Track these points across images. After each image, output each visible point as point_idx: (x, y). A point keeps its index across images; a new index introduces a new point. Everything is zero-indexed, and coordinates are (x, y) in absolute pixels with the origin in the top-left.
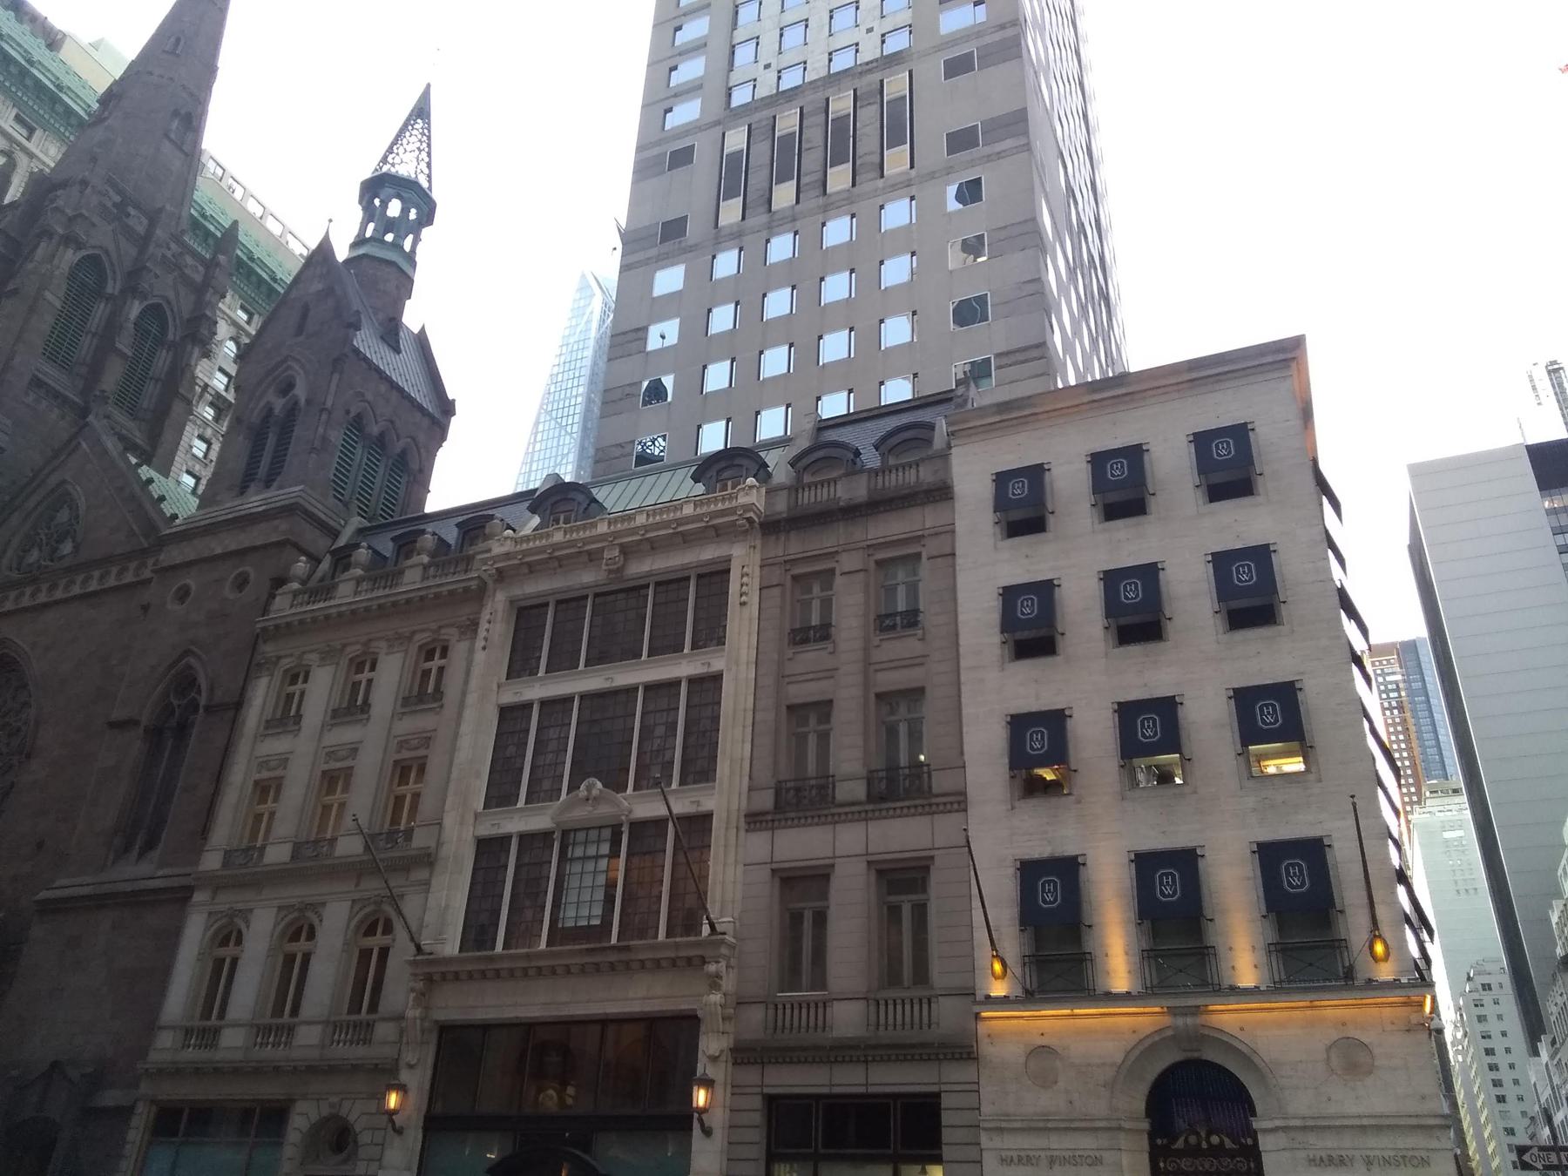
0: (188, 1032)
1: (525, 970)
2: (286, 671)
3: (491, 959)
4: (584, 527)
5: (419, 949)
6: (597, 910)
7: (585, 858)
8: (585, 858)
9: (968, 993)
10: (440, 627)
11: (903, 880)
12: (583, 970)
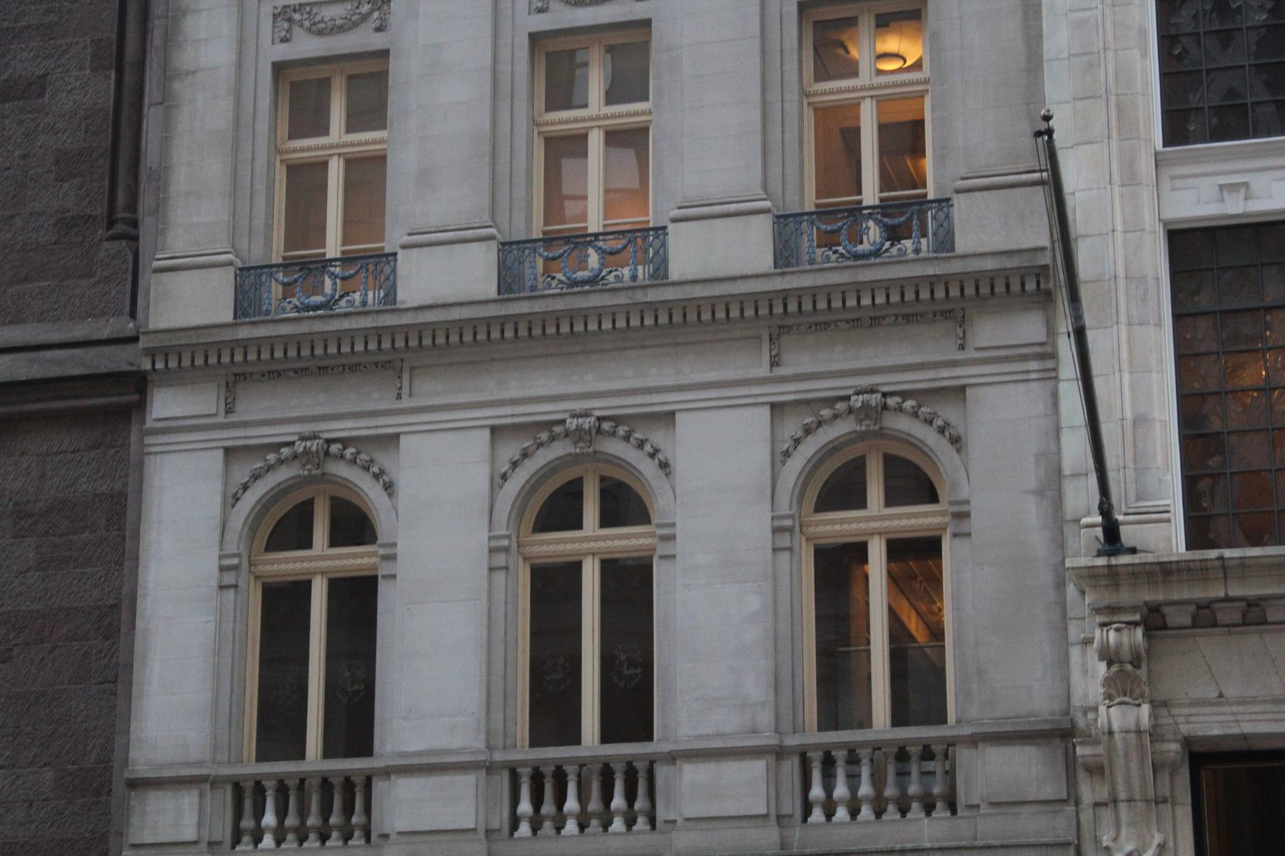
0: (246, 796)
5: (1111, 531)
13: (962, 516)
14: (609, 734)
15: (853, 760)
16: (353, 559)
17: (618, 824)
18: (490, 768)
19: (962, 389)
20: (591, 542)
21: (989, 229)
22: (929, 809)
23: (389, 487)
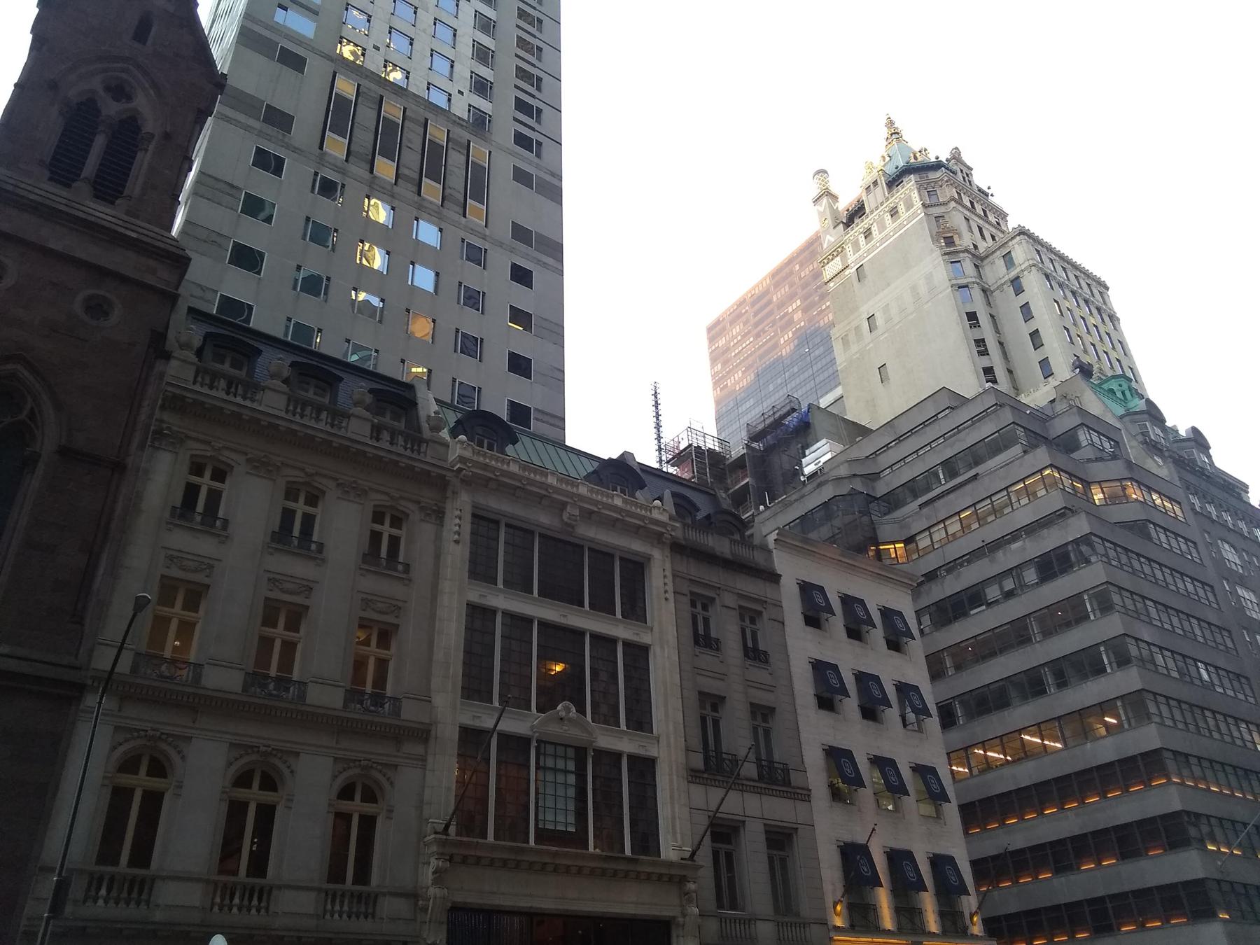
1: (660, 876)
2: (192, 456)
3: (522, 850)
4: (607, 496)
6: (571, 819)
7: (555, 770)
8: (555, 770)
9: (824, 923)
10: (402, 498)
11: (780, 840)
12: (593, 872)
13: (391, 811)
14: (355, 882)
15: (343, 895)
16: (156, 783)
17: (254, 911)
18: (207, 882)
19: (396, 766)
20: (357, 806)
21: (410, 713)
22: (366, 917)
23: (183, 758)
